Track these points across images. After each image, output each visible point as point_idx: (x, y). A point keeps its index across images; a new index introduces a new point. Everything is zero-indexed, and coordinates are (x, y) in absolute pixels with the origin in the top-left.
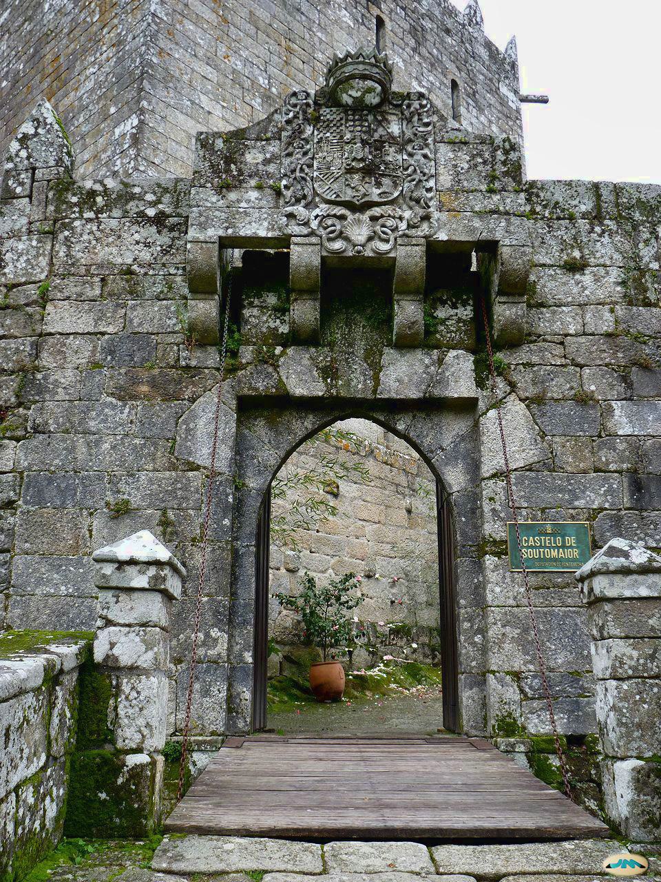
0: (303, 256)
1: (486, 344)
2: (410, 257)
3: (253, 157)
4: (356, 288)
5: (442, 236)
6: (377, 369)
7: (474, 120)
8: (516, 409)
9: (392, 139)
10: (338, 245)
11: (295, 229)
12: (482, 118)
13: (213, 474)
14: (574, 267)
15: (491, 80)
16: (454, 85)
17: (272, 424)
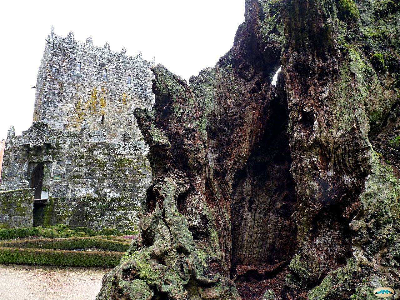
0: (31, 146)
1: (54, 154)
2: (42, 145)
3: (27, 134)
4: (38, 149)
5: (45, 143)
6: (42, 158)
7: (136, 82)
8: (56, 162)
9: (41, 131)
10: (35, 145)
11: (31, 143)
12: (139, 81)
13: (26, 171)
14: (64, 144)
15: (143, 70)
16: (130, 75)
17: (33, 165)
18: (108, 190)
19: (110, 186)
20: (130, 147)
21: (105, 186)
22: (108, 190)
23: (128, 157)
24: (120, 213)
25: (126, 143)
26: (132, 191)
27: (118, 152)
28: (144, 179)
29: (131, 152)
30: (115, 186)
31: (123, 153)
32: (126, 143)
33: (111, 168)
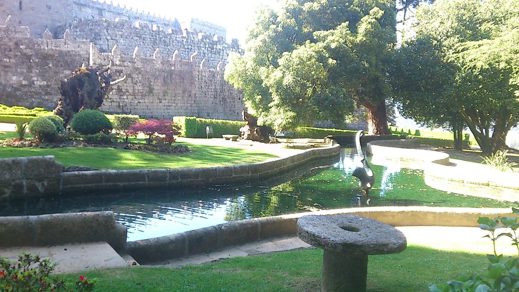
18: (35, 79)
19: (38, 75)
20: (51, 44)
21: (33, 75)
22: (35, 79)
23: (51, 52)
24: (47, 97)
25: (48, 40)
26: (55, 80)
27: (42, 47)
28: (65, 71)
29: (53, 48)
30: (42, 76)
31: (46, 48)
32: (48, 40)
33: (37, 60)
